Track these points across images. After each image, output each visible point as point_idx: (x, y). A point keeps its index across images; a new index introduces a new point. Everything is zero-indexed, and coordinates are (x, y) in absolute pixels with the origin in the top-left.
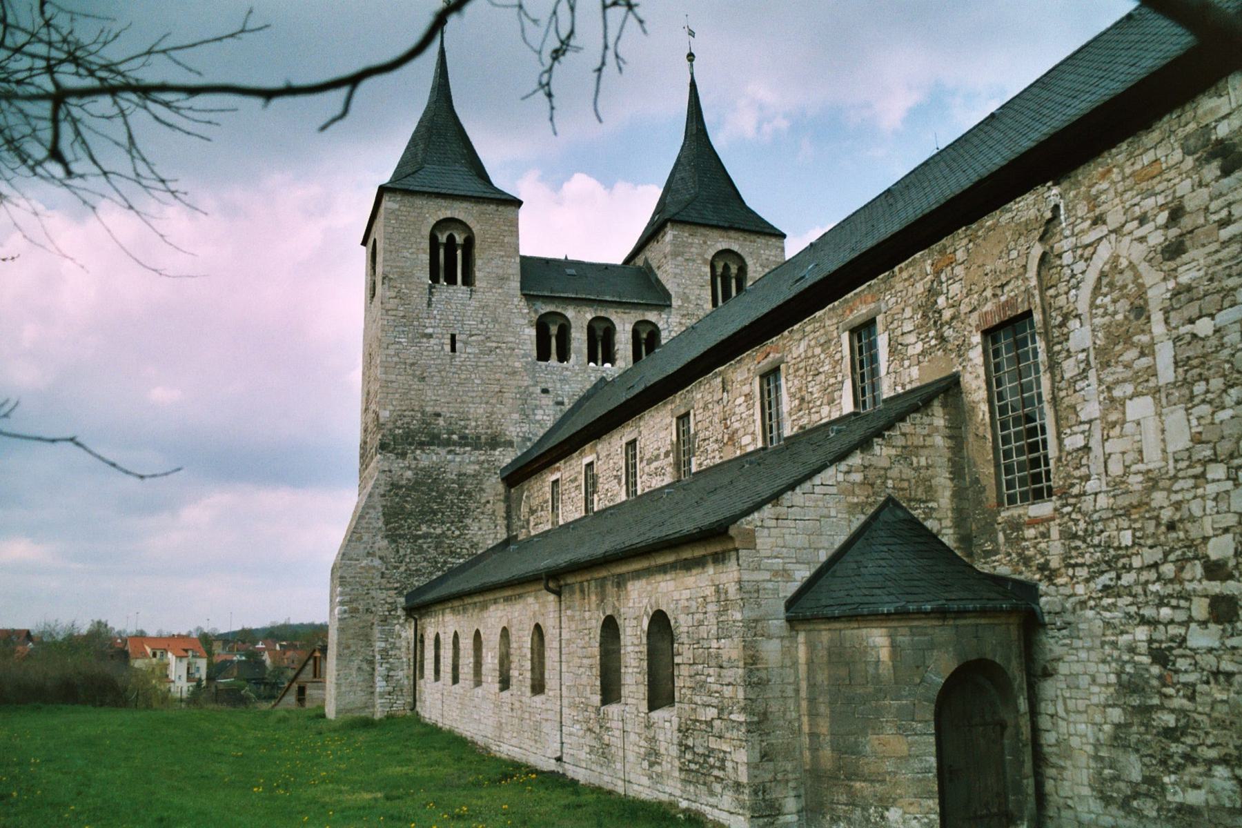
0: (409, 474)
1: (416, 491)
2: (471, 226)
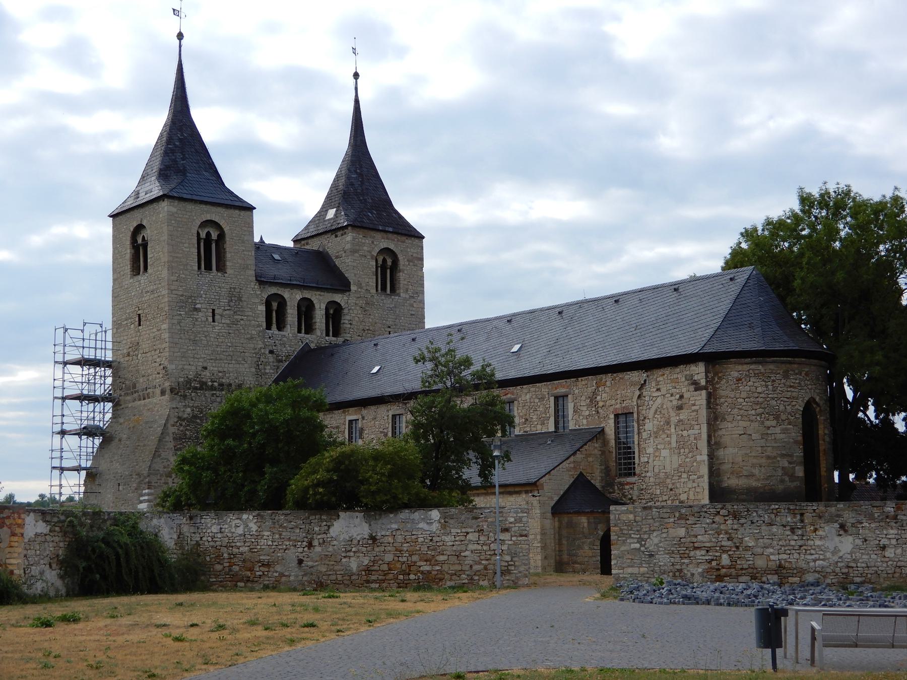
0: (189, 410)
1: (194, 422)
2: (223, 227)
